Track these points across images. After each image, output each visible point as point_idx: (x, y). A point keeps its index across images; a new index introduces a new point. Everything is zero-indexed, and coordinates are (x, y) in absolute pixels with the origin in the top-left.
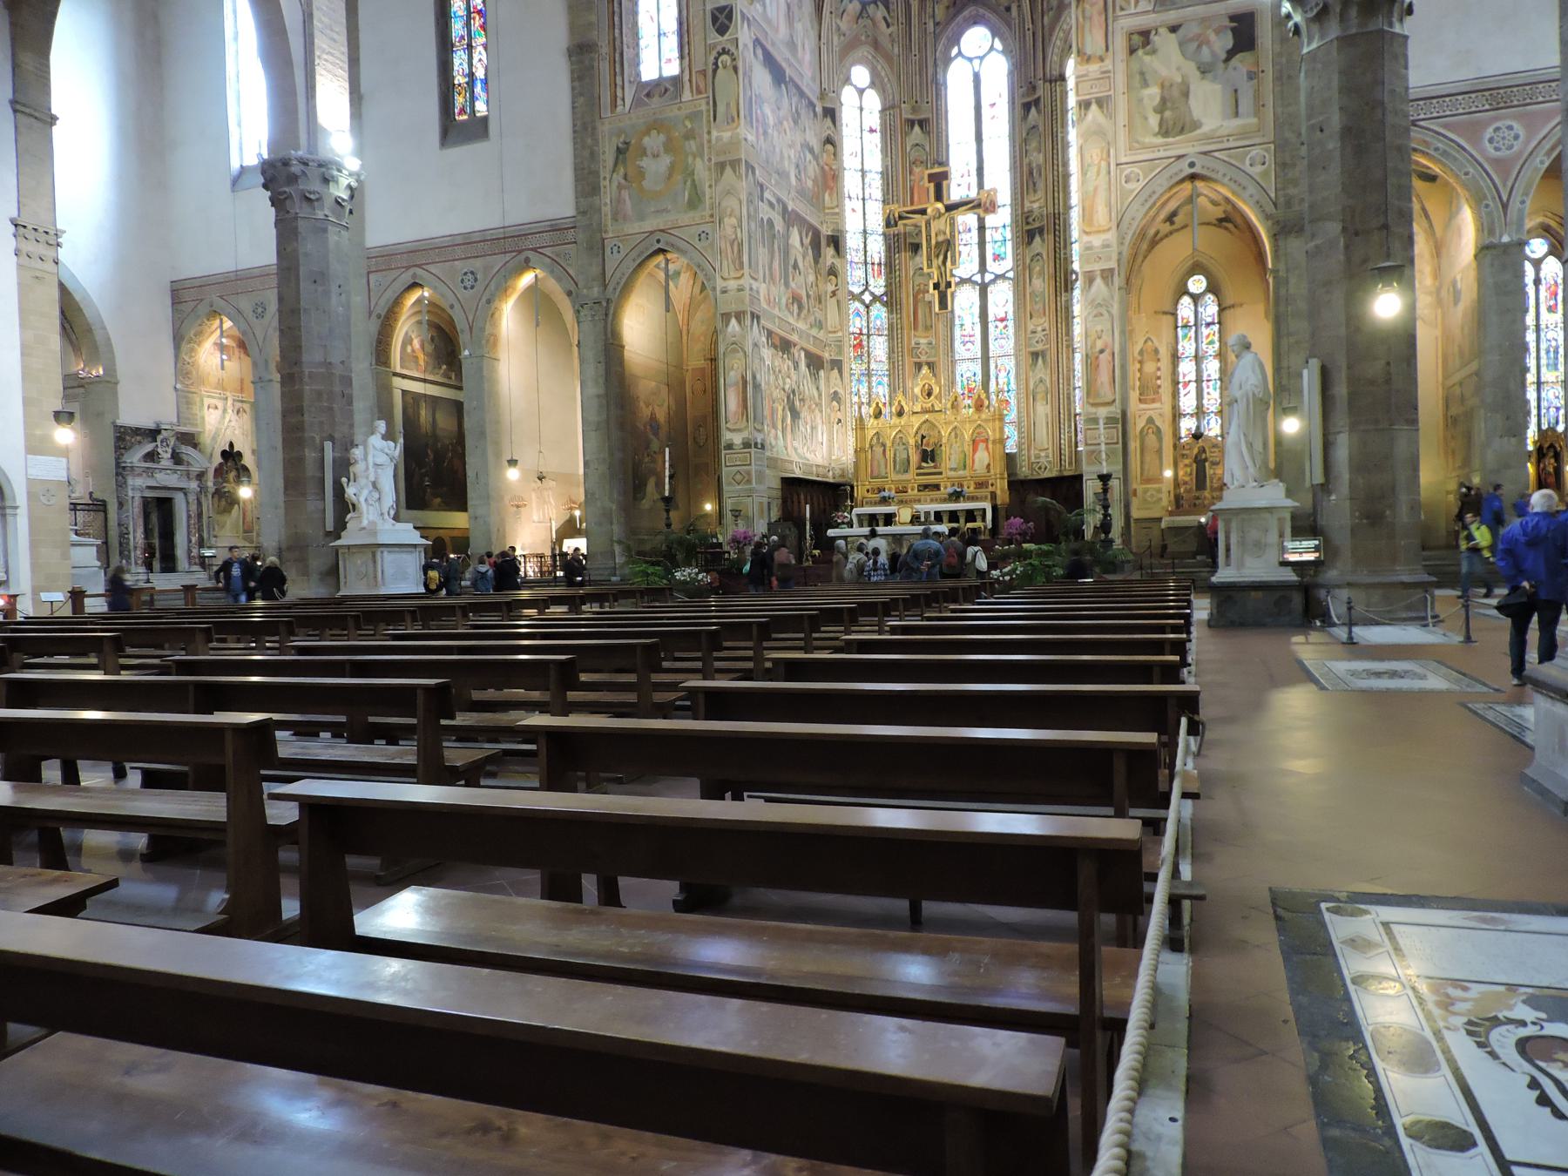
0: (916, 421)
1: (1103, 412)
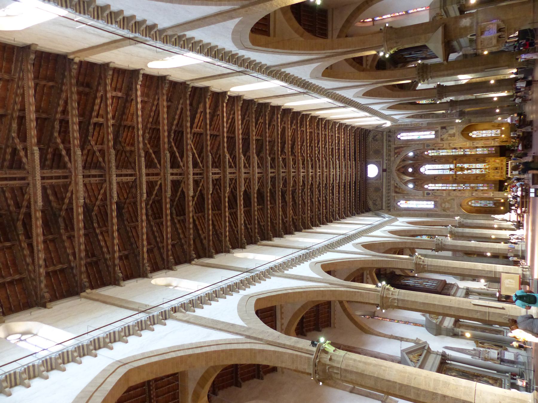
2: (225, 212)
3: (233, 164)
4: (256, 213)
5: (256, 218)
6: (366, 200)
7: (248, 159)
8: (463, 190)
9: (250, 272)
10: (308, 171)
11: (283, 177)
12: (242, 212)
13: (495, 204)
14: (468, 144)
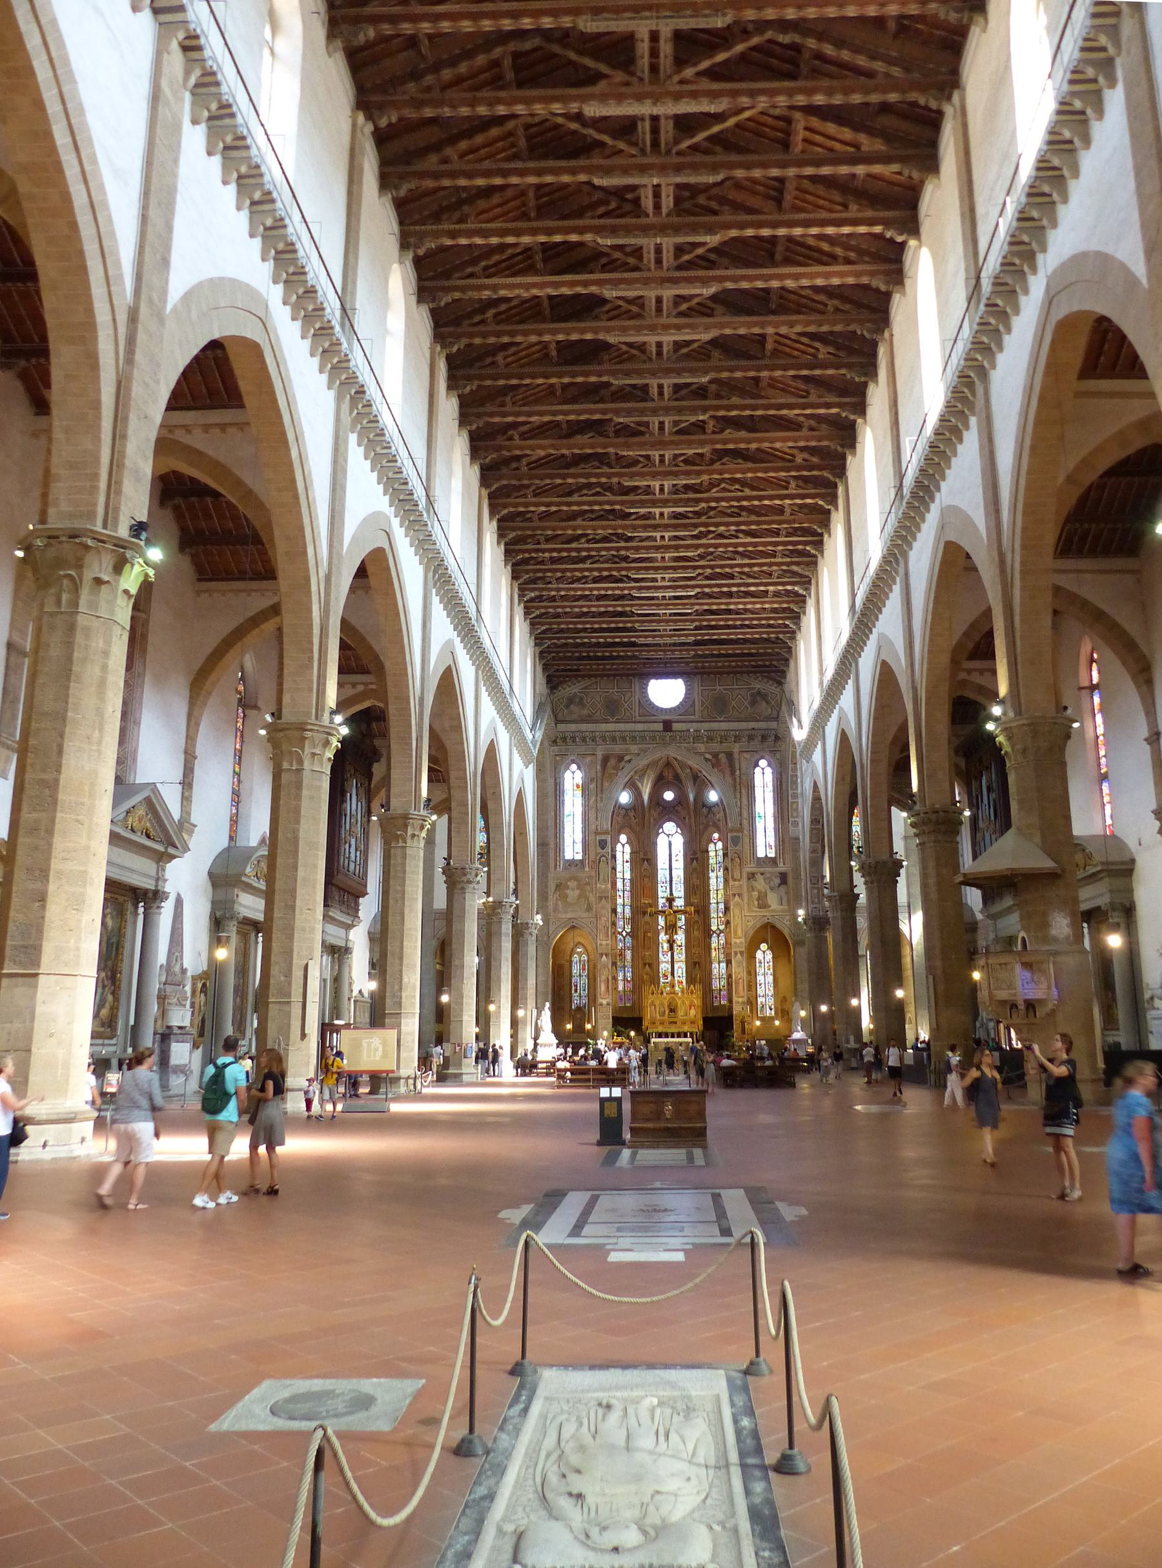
0: (668, 997)
1: (740, 1000)
2: (534, 232)
3: (686, 257)
4: (533, 338)
5: (519, 339)
6: (583, 677)
7: (703, 309)
8: (615, 933)
9: (342, 318)
10: (665, 503)
11: (647, 424)
12: (535, 292)
13: (579, 1009)
14: (738, 941)
